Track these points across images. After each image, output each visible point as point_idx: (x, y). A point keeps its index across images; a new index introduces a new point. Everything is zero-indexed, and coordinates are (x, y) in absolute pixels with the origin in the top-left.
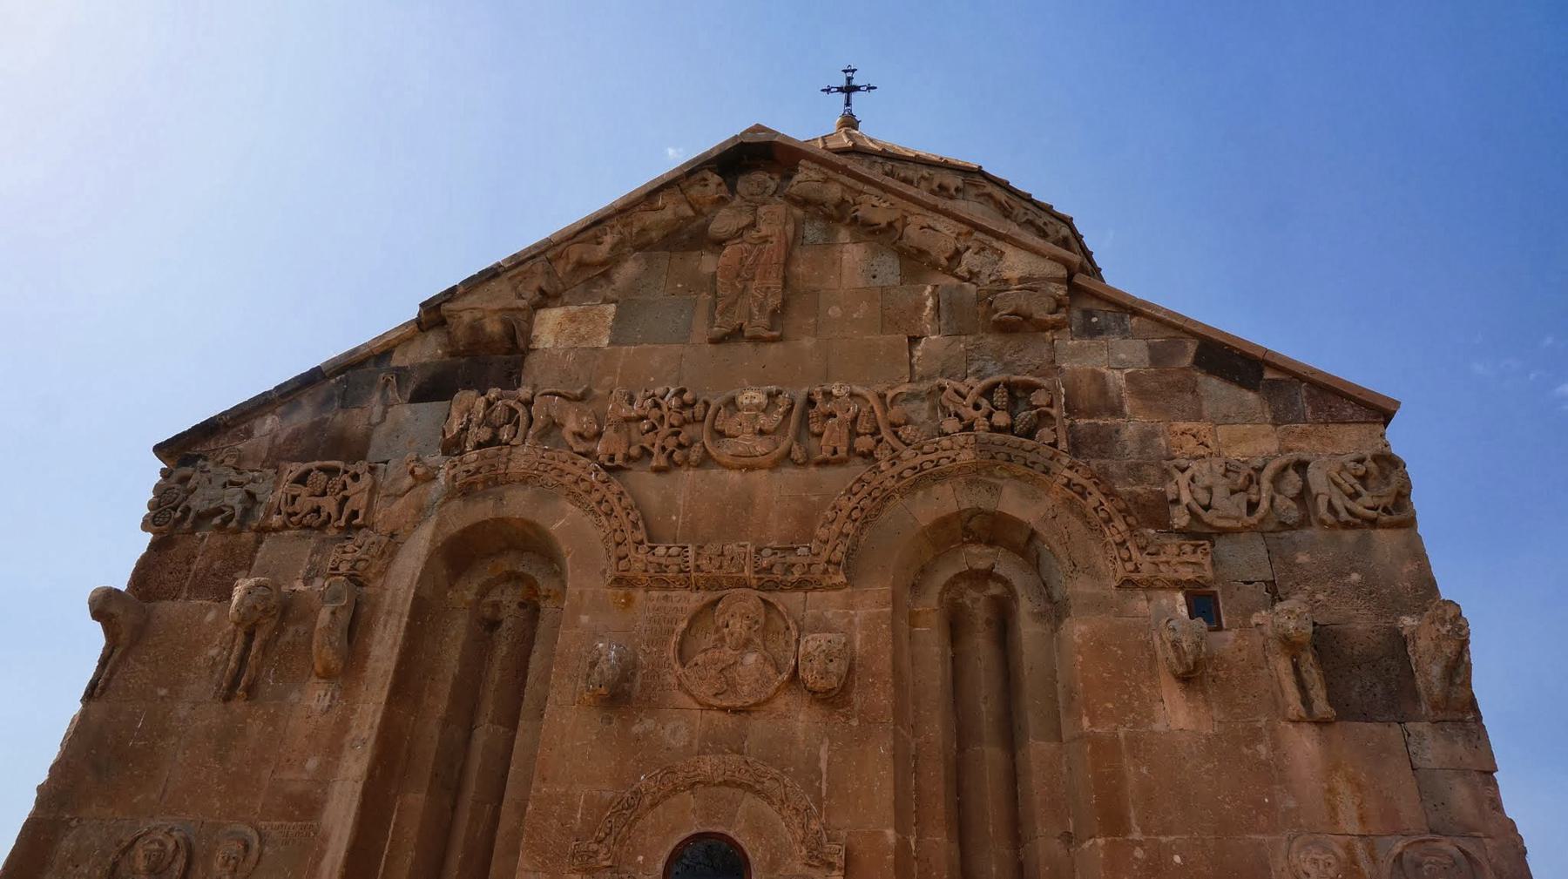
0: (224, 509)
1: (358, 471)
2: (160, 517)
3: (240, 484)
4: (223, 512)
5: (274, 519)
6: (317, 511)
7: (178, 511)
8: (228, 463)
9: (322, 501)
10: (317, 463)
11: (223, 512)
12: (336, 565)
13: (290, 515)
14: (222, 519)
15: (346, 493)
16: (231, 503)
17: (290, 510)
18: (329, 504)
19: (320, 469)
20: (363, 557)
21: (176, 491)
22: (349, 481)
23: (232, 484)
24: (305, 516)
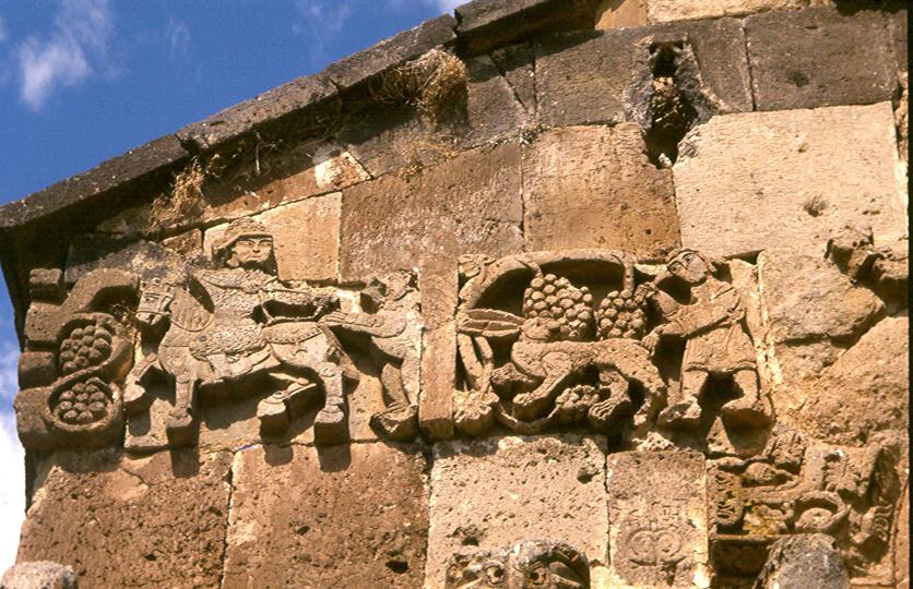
0: (282, 376)
1: (682, 273)
2: (73, 401)
3: (304, 311)
4: (284, 385)
5: (460, 401)
6: (589, 375)
7: (131, 379)
8: (244, 259)
9: (602, 351)
10: (547, 255)
11: (284, 385)
12: (733, 518)
13: (506, 391)
14: (286, 402)
15: (668, 329)
16: (302, 360)
17: (503, 373)
18: (630, 358)
19: (547, 268)
20: (817, 494)
21: (100, 330)
22: (664, 299)
23: (275, 308)
24: (558, 390)
